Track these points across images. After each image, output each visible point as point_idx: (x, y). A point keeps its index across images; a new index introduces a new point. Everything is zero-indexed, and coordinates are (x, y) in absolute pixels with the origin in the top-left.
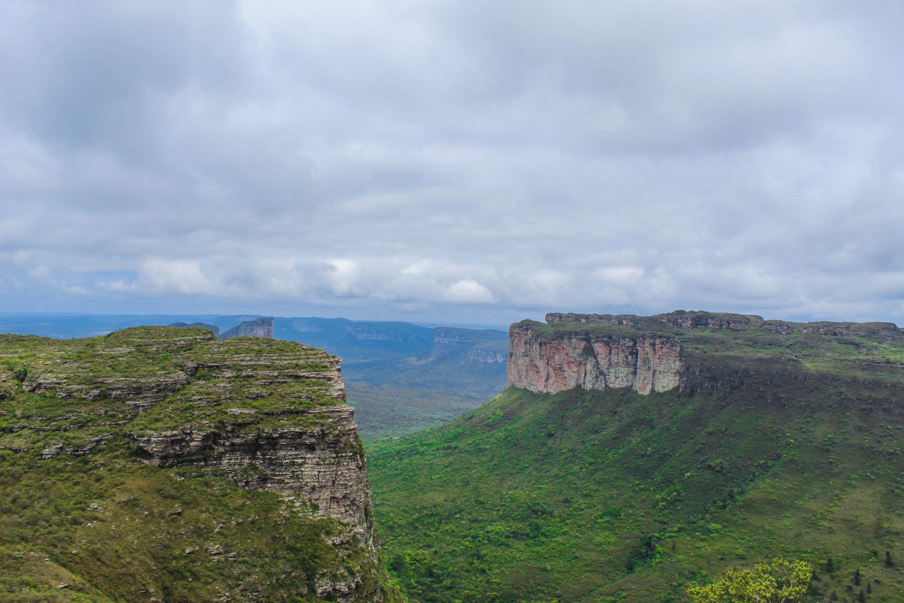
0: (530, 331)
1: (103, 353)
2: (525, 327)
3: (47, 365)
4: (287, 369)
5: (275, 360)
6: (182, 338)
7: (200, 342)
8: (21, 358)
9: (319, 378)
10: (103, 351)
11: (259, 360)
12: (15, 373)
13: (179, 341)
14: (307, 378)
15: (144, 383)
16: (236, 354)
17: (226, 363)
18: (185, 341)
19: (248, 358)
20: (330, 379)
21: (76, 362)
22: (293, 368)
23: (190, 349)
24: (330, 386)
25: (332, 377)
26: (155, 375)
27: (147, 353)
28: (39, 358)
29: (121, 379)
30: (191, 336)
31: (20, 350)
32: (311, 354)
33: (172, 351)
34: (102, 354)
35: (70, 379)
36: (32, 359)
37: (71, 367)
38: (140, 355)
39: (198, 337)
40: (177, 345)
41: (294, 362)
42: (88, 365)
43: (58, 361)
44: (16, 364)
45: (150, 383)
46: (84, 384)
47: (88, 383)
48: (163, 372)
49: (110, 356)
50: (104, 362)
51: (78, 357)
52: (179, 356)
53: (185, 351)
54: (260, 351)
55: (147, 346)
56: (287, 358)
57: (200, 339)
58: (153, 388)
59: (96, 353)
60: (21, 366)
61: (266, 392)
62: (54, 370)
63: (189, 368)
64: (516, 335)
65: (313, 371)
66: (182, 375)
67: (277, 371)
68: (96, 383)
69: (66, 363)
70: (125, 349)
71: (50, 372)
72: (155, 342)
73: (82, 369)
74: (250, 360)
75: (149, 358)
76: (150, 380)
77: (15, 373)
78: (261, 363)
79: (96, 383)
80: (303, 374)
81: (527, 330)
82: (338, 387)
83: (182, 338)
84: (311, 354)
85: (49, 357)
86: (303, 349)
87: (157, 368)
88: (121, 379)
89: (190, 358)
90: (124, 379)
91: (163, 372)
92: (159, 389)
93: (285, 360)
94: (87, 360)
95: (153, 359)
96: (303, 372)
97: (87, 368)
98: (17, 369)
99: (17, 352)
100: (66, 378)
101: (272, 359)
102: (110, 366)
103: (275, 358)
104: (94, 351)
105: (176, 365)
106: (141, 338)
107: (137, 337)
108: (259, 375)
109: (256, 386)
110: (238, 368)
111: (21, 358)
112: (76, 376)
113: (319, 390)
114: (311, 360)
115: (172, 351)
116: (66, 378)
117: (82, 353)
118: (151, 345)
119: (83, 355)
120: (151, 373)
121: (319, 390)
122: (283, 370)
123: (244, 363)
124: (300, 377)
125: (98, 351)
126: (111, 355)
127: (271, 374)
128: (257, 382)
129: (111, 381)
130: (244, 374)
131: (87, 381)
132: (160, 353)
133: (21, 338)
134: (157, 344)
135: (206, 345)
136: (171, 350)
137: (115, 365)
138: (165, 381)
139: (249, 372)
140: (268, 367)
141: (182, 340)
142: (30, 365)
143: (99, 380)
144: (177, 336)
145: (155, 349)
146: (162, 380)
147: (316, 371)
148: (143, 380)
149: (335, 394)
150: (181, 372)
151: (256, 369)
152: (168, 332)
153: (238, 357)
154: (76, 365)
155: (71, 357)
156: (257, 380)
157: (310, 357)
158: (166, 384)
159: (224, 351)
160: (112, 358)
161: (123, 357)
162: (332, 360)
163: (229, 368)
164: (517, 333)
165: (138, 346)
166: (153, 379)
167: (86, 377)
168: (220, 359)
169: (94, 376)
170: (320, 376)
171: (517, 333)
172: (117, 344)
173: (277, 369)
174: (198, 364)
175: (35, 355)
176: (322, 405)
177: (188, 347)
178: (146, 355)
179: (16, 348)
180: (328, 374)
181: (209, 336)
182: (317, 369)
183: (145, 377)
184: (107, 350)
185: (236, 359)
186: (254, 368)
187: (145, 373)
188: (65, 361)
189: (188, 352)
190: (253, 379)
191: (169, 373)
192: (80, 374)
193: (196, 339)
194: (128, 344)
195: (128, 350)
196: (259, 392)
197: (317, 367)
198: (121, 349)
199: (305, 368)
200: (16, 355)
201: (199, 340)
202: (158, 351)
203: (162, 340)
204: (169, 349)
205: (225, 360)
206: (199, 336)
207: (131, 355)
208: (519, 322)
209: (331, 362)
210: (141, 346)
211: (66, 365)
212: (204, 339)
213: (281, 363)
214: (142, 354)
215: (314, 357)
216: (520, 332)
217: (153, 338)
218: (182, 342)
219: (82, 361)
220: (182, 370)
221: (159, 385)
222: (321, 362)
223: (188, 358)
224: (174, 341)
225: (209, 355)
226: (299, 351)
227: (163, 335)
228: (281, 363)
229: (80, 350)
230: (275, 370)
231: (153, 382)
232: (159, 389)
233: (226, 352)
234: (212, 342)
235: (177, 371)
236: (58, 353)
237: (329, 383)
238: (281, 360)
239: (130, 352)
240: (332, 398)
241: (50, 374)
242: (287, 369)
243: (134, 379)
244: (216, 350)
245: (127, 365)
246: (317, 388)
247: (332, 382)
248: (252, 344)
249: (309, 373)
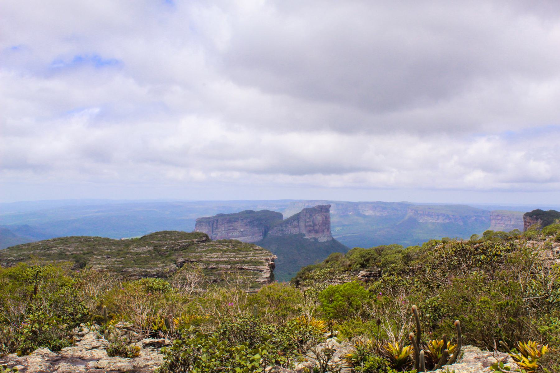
0: (539, 221)
1: (133, 251)
2: (535, 217)
3: (98, 259)
4: (237, 264)
5: (232, 257)
6: (184, 241)
7: (196, 244)
8: (84, 254)
9: (255, 270)
10: (133, 250)
11: (222, 257)
12: (80, 264)
13: (181, 243)
14: (247, 269)
15: (149, 272)
16: (210, 253)
17: (202, 259)
18: (185, 243)
19: (216, 256)
20: (261, 271)
21: (115, 257)
22: (241, 263)
23: (185, 249)
24: (261, 275)
25: (263, 269)
26: (157, 267)
27: (160, 251)
28: (94, 254)
29: (137, 269)
30: (191, 239)
31: (85, 248)
32: (257, 254)
33: (176, 250)
34: (131, 252)
35: (109, 268)
36: (90, 255)
37: (111, 260)
38: (154, 253)
39: (195, 240)
40: (180, 245)
41: (243, 259)
42: (121, 259)
43: (105, 256)
44: (80, 258)
45: (152, 272)
46: (116, 272)
47: (119, 271)
48: (162, 265)
49: (136, 254)
50: (131, 257)
51: (118, 253)
52: (177, 254)
53: (182, 250)
54: (225, 251)
55: (161, 246)
56: (240, 256)
57: (196, 241)
58: (154, 274)
59: (128, 251)
60: (83, 259)
61: (220, 279)
62: (101, 262)
63: (179, 262)
64: (528, 223)
65: (252, 266)
66: (173, 266)
67: (230, 265)
68: (123, 271)
69: (109, 257)
70: (146, 249)
71: (98, 264)
72: (166, 243)
73: (117, 262)
74: (216, 258)
75: (160, 255)
76: (153, 270)
77: (80, 264)
78: (223, 259)
79: (123, 271)
80: (244, 267)
81: (537, 219)
82: (265, 276)
83: (184, 241)
84: (257, 254)
85: (100, 254)
86: (255, 250)
87: (160, 262)
88: (137, 269)
89: (182, 255)
90: (138, 269)
91: (162, 265)
92: (157, 276)
93: (239, 257)
94: (122, 256)
95: (162, 256)
96: (246, 266)
97: (121, 261)
98: (81, 262)
99: (82, 250)
100: (106, 268)
101: (230, 257)
102: (134, 260)
103: (233, 256)
104: (128, 250)
105: (172, 260)
106: (159, 241)
107: (157, 239)
108: (219, 267)
109: (215, 274)
110: (208, 263)
111: (84, 254)
112: (112, 266)
113: (253, 278)
114: (255, 258)
115: (176, 250)
116: (106, 268)
117: (120, 251)
118: (163, 246)
119: (121, 252)
120: (154, 266)
121: (253, 278)
122: (234, 264)
123: (212, 259)
124: (243, 269)
125: (130, 250)
126: (137, 252)
127: (226, 267)
128: (216, 272)
129: (130, 270)
130: (210, 267)
131: (118, 270)
132: (168, 252)
133: (89, 240)
134: (167, 245)
135: (196, 246)
136: (175, 249)
137: (137, 260)
138: (161, 271)
139: (213, 266)
140: (225, 262)
141: (183, 242)
142: (88, 259)
143: (125, 269)
144: (181, 239)
145: (165, 248)
146: (160, 270)
147: (254, 265)
148: (148, 270)
149: (262, 281)
150: (173, 265)
151: (218, 264)
152: (178, 236)
153: (210, 255)
154: (115, 259)
155: (113, 254)
156: (217, 271)
157: (256, 255)
158: (162, 273)
159: (204, 251)
160: (137, 255)
161: (143, 254)
162: (268, 257)
163: (202, 262)
164: (529, 222)
165: (155, 246)
166: (155, 269)
167: (118, 267)
168: (199, 256)
169: (123, 267)
170: (256, 269)
171: (529, 222)
172: (143, 245)
173: (231, 264)
174: (185, 259)
175: (93, 252)
176: (251, 288)
177: (184, 248)
178: (158, 253)
179: (83, 247)
180: (261, 267)
181: (204, 239)
182: (254, 264)
183: (151, 268)
184: (136, 249)
185: (208, 257)
186: (217, 263)
187: (151, 266)
188: (109, 256)
189: (184, 251)
190: (215, 270)
191: (166, 266)
192: (115, 266)
193: (193, 241)
194: (150, 244)
195: (148, 249)
196: (215, 278)
197: (255, 262)
198: (144, 248)
199: (248, 263)
200: (82, 252)
201: (195, 242)
202: (167, 250)
203: (171, 242)
204: (174, 248)
205: (202, 257)
206: (196, 239)
207: (149, 253)
208: (531, 211)
209: (267, 259)
210: (157, 246)
211: (109, 259)
212: (198, 241)
213: (234, 260)
214: (156, 252)
215: (259, 255)
216: (531, 221)
217: (166, 241)
218: (183, 244)
219: (119, 257)
220: (175, 263)
221: (158, 273)
222: (260, 259)
223: (181, 256)
224: (179, 243)
225: (193, 254)
226: (251, 251)
227: (173, 238)
228: (234, 260)
229: (120, 249)
230: (229, 264)
231: (155, 271)
232: (157, 276)
233: (205, 251)
234: (202, 244)
235: (172, 264)
236: (106, 251)
237: (261, 273)
238: (235, 257)
239: (149, 251)
240: (259, 283)
241: (98, 265)
242: (237, 263)
243: (144, 269)
244: (199, 250)
245: (144, 260)
246: (251, 276)
247: (262, 273)
248: (225, 245)
249: (249, 267)
